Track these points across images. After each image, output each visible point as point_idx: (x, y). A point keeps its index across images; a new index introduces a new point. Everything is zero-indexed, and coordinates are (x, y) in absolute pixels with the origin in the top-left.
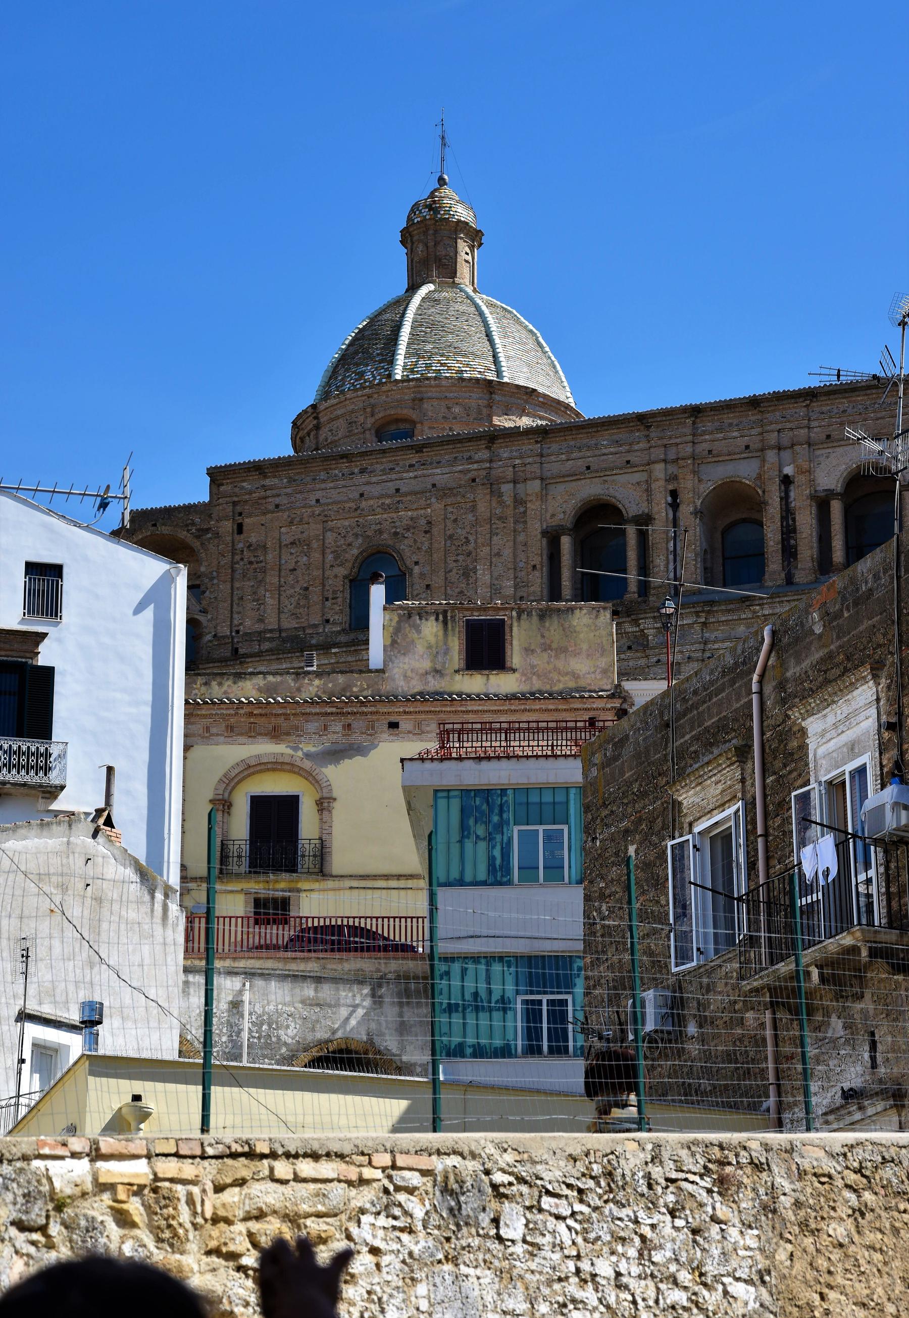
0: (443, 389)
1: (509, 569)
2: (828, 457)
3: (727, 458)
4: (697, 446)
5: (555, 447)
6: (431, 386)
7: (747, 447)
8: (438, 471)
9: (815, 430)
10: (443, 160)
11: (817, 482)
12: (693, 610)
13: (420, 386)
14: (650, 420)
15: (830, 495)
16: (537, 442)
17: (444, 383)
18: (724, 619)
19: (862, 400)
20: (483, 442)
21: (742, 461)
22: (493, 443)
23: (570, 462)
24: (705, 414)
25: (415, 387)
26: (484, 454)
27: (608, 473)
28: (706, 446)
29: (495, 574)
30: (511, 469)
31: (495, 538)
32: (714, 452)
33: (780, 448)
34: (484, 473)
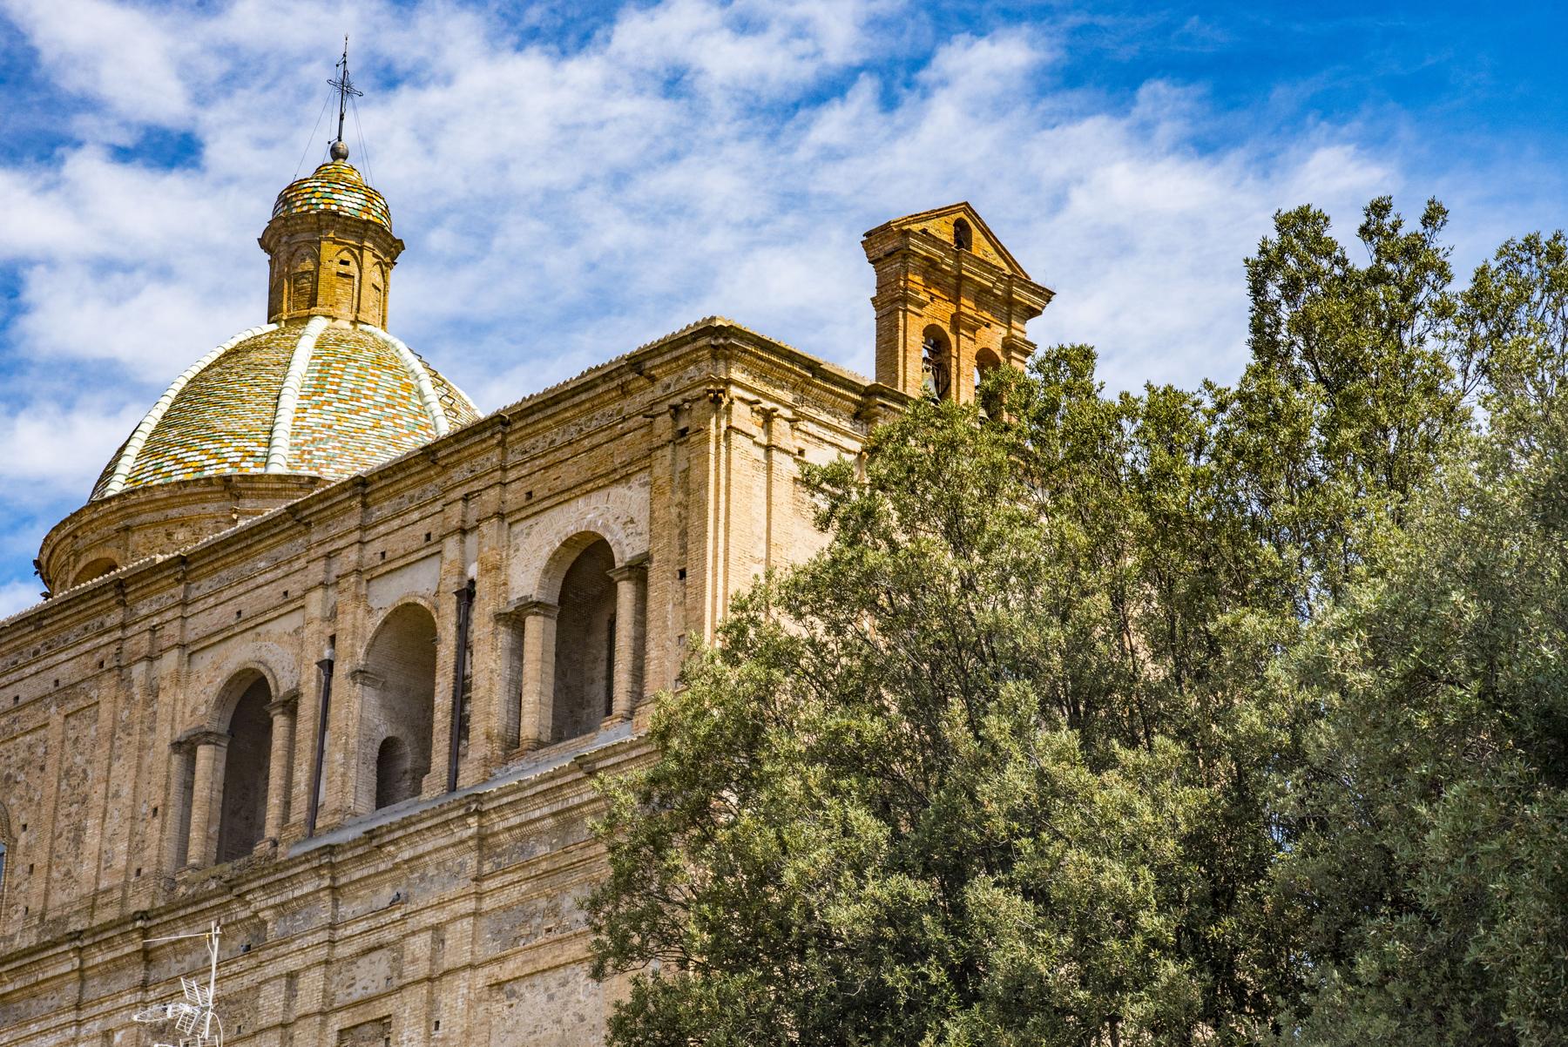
0: (161, 503)
1: (126, 819)
2: (528, 534)
3: (401, 562)
4: (368, 547)
5: (206, 585)
6: (142, 504)
7: (428, 536)
8: (63, 656)
9: (513, 486)
10: (342, 118)
11: (511, 585)
12: (307, 866)
13: (125, 507)
14: (306, 512)
15: (529, 606)
16: (179, 581)
17: (159, 495)
18: (357, 876)
19: (574, 417)
20: (110, 594)
21: (421, 564)
22: (125, 595)
23: (220, 608)
24: (375, 487)
25: (118, 510)
26: (115, 617)
27: (260, 620)
28: (378, 546)
29: (108, 833)
30: (147, 635)
31: (116, 765)
32: (388, 555)
33: (464, 532)
34: (113, 649)
